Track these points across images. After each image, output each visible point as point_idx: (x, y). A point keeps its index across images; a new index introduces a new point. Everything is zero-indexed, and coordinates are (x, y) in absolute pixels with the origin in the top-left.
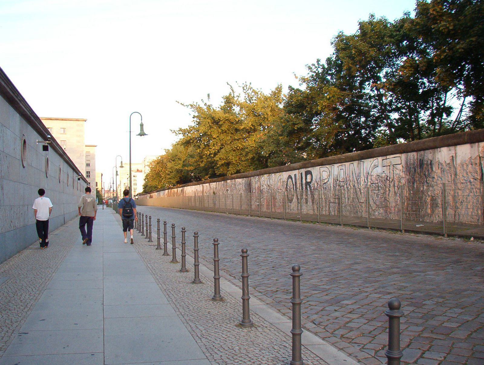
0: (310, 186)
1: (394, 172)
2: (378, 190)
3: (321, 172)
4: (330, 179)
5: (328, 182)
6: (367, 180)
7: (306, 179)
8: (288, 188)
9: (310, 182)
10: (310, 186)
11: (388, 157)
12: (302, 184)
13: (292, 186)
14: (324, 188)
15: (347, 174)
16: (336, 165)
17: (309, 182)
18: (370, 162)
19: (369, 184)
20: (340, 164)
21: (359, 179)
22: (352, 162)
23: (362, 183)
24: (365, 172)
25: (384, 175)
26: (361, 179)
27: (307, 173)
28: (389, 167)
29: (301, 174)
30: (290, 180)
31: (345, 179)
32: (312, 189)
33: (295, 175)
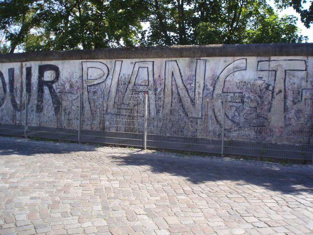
0: (51, 88)
1: (287, 80)
2: (243, 102)
4: (109, 82)
5: (104, 84)
7: (41, 74)
9: (53, 82)
10: (51, 88)
11: (273, 58)
12: (29, 84)
14: (88, 92)
15: (156, 76)
18: (225, 61)
19: (218, 91)
20: (137, 60)
22: (173, 59)
23: (199, 90)
25: (260, 82)
26: (197, 85)
27: (42, 70)
28: (274, 72)
29: (29, 70)
31: (151, 82)
33: (11, 71)
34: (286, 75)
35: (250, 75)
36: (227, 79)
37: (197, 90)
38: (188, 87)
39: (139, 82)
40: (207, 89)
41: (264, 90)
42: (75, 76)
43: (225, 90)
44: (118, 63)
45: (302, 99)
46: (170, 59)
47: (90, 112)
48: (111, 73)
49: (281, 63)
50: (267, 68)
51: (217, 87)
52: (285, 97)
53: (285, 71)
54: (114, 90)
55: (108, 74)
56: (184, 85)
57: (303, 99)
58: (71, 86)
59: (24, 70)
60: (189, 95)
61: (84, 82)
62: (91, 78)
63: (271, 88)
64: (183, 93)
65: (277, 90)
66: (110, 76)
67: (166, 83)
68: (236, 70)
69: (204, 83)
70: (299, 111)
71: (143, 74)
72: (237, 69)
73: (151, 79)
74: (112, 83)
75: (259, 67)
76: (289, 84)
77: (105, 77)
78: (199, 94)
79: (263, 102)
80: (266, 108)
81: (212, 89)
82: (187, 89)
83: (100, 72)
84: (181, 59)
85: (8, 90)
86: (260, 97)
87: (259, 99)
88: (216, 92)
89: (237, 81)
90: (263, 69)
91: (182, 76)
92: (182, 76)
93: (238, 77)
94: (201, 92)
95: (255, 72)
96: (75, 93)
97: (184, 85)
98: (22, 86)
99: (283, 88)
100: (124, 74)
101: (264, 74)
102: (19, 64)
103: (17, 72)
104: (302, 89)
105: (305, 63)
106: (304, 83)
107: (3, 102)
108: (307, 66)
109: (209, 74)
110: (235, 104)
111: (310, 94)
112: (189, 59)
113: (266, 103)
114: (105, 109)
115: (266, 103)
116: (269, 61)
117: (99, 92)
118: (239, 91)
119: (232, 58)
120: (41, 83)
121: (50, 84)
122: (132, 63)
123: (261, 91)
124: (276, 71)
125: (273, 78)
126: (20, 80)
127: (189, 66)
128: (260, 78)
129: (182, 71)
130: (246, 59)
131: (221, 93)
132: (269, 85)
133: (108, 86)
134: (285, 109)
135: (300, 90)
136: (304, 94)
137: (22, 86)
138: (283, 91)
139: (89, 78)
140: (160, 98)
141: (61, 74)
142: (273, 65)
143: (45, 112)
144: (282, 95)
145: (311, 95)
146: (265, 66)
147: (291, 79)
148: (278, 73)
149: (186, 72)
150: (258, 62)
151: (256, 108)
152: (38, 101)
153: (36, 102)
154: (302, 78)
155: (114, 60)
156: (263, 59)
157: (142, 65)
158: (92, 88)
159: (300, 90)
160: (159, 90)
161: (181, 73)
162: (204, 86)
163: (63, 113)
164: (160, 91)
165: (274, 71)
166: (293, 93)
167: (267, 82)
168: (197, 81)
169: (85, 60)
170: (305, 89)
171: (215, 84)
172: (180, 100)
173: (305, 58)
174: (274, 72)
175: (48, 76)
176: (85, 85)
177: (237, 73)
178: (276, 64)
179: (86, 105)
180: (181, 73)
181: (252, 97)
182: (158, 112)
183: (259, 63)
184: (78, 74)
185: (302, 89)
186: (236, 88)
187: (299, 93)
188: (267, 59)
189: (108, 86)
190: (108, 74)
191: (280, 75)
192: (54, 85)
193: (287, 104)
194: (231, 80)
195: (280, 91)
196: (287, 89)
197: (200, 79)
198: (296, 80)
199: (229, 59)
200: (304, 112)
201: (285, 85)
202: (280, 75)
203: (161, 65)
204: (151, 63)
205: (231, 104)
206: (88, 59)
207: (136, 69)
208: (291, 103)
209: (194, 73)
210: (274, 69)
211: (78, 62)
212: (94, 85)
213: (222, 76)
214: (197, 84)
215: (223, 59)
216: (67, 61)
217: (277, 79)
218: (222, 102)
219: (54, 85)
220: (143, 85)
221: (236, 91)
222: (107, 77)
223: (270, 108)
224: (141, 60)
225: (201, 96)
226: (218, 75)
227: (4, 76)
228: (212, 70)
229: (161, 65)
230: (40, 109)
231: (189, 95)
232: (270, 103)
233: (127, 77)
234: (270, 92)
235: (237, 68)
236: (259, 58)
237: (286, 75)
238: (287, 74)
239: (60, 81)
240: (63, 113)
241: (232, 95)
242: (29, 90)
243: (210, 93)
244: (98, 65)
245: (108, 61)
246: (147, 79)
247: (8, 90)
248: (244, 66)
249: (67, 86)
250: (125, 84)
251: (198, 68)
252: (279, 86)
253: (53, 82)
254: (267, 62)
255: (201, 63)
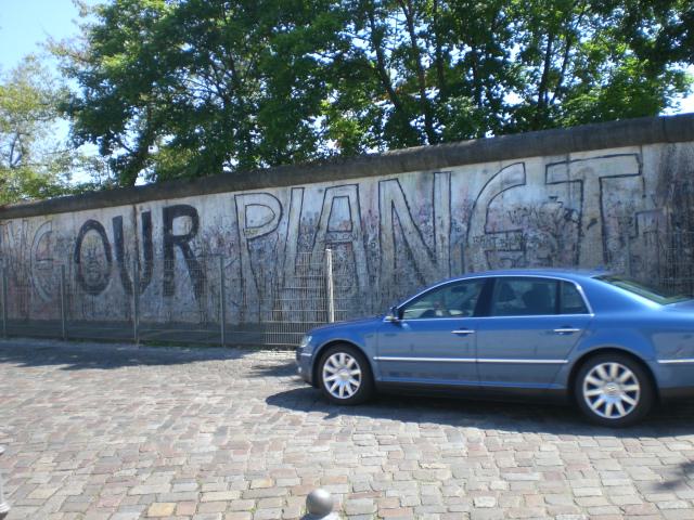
0: (185, 248)
1: (605, 197)
2: (523, 248)
3: (241, 208)
4: (283, 229)
5: (275, 235)
6: (469, 225)
8: (84, 253)
10: (185, 248)
11: (573, 156)
12: (148, 245)
13: (101, 249)
14: (250, 252)
16: (312, 190)
17: (179, 238)
18: (485, 172)
19: (477, 231)
20: (330, 184)
21: (425, 222)
22: (392, 176)
24: (457, 199)
25: (552, 207)
26: (438, 223)
27: (169, 215)
28: (578, 184)
29: (147, 217)
30: (93, 233)
31: (357, 224)
32: (197, 253)
33: (118, 222)
34: (601, 187)
35: (532, 194)
36: (492, 206)
37: (438, 233)
38: (422, 227)
39: (336, 225)
40: (458, 230)
41: (562, 222)
42: (224, 221)
43: (490, 229)
44: (297, 193)
45: (637, 233)
46: (386, 177)
47: (254, 292)
48: (286, 212)
49: (590, 164)
50: (565, 178)
51: (474, 224)
52: (604, 233)
53: (600, 178)
54: (292, 243)
55: (281, 215)
56: (415, 225)
57: (641, 232)
58: (220, 242)
59: (139, 218)
60: (424, 243)
61: (241, 233)
62: (253, 225)
63: (575, 216)
64: (413, 240)
65: (586, 220)
66: (285, 219)
67: (383, 223)
68: (506, 186)
69: (451, 218)
70: (634, 259)
71: (342, 210)
72: (509, 184)
73: (355, 218)
74: (289, 230)
75: (549, 176)
76: (610, 205)
77: (275, 222)
78: (443, 239)
79: (561, 246)
80: (569, 257)
81: (466, 229)
82: (419, 231)
83: (266, 212)
84: (406, 174)
85: (114, 258)
86: (555, 236)
87: (554, 241)
88: (473, 234)
89: (510, 208)
90: (556, 180)
91: (409, 209)
92: (409, 209)
93: (511, 199)
94: (446, 236)
95: (543, 189)
96: (228, 254)
97: (415, 225)
98: (136, 249)
99: (598, 214)
100: (308, 214)
101: (561, 188)
102: (129, 208)
103: (127, 223)
104: (637, 214)
105: (638, 159)
106: (638, 201)
107: (108, 280)
108: (641, 166)
109: (457, 199)
110: (510, 255)
111: (653, 221)
112: (417, 174)
113: (568, 247)
114: (280, 281)
115: (568, 247)
116: (567, 162)
117: (269, 251)
118: (516, 228)
119: (497, 164)
120: (170, 241)
121: (183, 241)
122: (320, 191)
123: (556, 223)
124: (582, 182)
125: (578, 196)
126: (134, 236)
127: (421, 188)
128: (552, 198)
129: (409, 199)
130: (524, 164)
131: (482, 234)
132: (571, 211)
133: (282, 238)
134: (605, 255)
135: (633, 215)
136: (641, 223)
137: (136, 249)
138: (599, 220)
139: (249, 224)
140: (374, 254)
141: (201, 221)
142: (575, 169)
143: (179, 294)
144: (598, 228)
145: (655, 224)
146: (559, 172)
147: (611, 194)
148: (586, 186)
149: (417, 200)
150: (547, 166)
151: (549, 258)
152: (166, 275)
153: (162, 277)
154: (634, 192)
155: (289, 188)
156: (555, 159)
157: (339, 192)
158: (254, 244)
159: (633, 215)
160: (370, 238)
161: (407, 203)
162: (451, 224)
163: (209, 294)
164: (374, 239)
165: (578, 181)
166: (620, 223)
167: (566, 205)
168: (436, 215)
169: (240, 192)
170: (642, 212)
171: (470, 218)
172: (410, 255)
173: (636, 150)
174: (578, 184)
175: (180, 226)
176: (243, 239)
177: (508, 194)
178: (581, 167)
179: (248, 275)
180: (407, 203)
181: (542, 238)
182: (372, 279)
183: (549, 169)
184: (228, 220)
185: (637, 214)
186: (509, 222)
187: (630, 221)
188: (562, 158)
189: (282, 238)
190: (281, 215)
191: (591, 188)
192: (191, 243)
193: (610, 246)
194: (499, 207)
195: (594, 222)
196: (605, 215)
197: (441, 210)
198: (622, 196)
199: (493, 166)
200: (643, 258)
201: (601, 208)
202: (591, 188)
203: (372, 190)
204: (354, 189)
205: (502, 254)
206: (243, 190)
207: (328, 201)
208: (617, 243)
209: (430, 200)
210: (578, 178)
211: (229, 195)
212: (259, 237)
213: (482, 201)
214: (437, 220)
215: (480, 167)
216: (210, 196)
217: (585, 197)
218: (486, 252)
219: (191, 243)
220: (341, 232)
221: (509, 228)
222: (280, 220)
223: (578, 256)
224: (337, 183)
225: (446, 243)
226: (474, 199)
227: (107, 231)
228: (462, 190)
229: (372, 190)
230: (169, 290)
231: (424, 243)
232: (576, 247)
233: (313, 217)
234: (575, 225)
235: (507, 182)
236: (548, 160)
237: (601, 187)
238: (604, 185)
239: (201, 235)
240: (209, 294)
241: (502, 236)
242: (149, 255)
243: (461, 236)
244: (263, 199)
245: (280, 189)
246: (347, 218)
247: (114, 258)
248: (519, 176)
249: (214, 243)
250: (311, 231)
251: (437, 189)
252: (591, 210)
253: (188, 237)
254: (564, 165)
255: (441, 180)
